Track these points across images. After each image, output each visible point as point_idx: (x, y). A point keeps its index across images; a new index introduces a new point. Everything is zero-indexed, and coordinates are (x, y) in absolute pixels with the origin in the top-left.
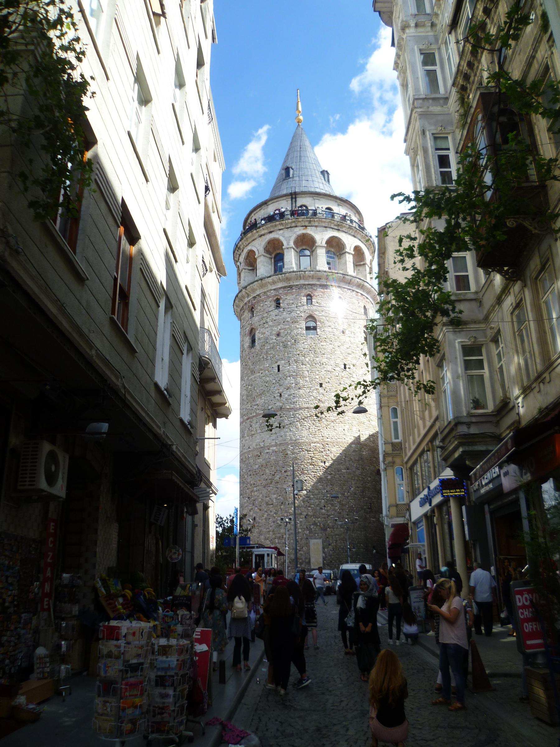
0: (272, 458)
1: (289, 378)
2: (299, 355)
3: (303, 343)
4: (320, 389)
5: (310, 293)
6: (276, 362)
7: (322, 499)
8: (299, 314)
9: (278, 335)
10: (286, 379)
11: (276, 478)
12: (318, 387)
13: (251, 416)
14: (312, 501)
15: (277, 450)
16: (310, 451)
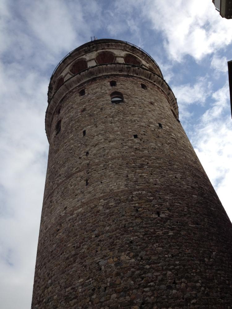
0: (76, 224)
1: (96, 137)
2: (106, 117)
3: (110, 109)
4: (135, 139)
5: (114, 80)
6: (81, 130)
7: (167, 269)
8: (103, 92)
9: (84, 110)
10: (93, 139)
11: (83, 250)
12: (133, 138)
13: (52, 190)
14: (150, 275)
15: (83, 211)
16: (133, 200)
